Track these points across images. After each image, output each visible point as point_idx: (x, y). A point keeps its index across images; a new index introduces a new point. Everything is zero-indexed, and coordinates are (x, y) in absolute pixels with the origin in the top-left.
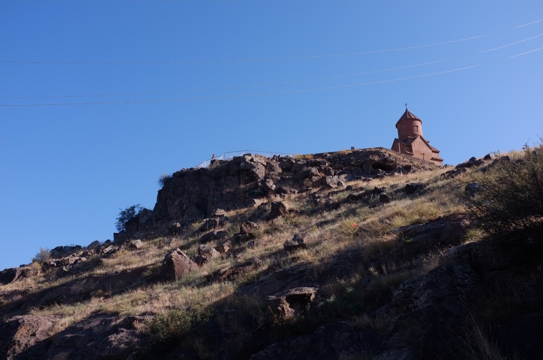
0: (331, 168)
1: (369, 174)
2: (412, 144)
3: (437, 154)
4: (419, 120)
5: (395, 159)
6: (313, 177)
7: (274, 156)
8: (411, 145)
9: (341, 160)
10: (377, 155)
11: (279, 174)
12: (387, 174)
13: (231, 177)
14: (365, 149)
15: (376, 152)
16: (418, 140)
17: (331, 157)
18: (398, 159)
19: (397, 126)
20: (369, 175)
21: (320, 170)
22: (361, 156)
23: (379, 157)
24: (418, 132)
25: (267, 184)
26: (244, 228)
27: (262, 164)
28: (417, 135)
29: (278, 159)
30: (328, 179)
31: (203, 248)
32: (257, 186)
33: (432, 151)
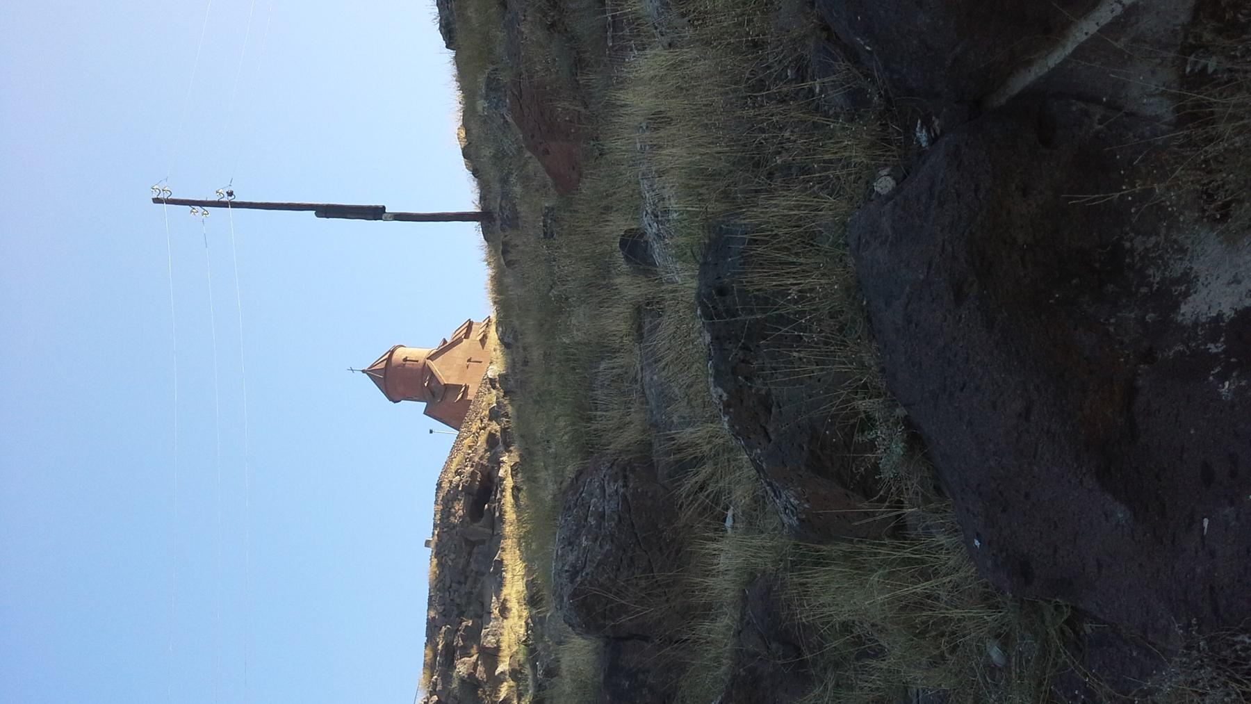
0: (464, 624)
1: (493, 532)
3: (474, 326)
4: (392, 352)
5: (470, 461)
6: (477, 675)
8: (445, 384)
9: (450, 587)
10: (453, 503)
12: (498, 496)
14: (435, 526)
15: (446, 504)
16: (434, 365)
18: (469, 454)
19: (395, 402)
20: (495, 533)
23: (460, 500)
24: (417, 361)
28: (425, 363)
30: (489, 642)
33: (465, 338)
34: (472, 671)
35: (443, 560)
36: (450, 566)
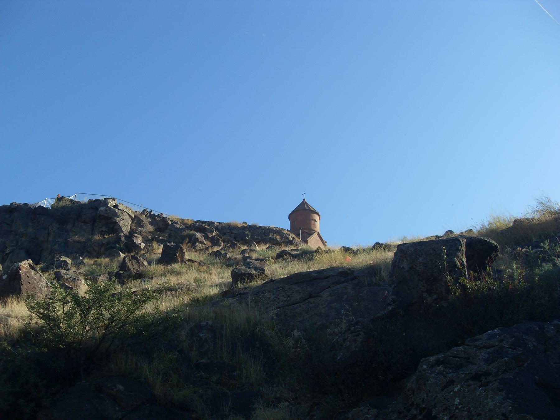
2: (308, 239)
4: (318, 214)
6: (198, 243)
7: (144, 209)
8: (307, 241)
10: (279, 235)
11: (150, 232)
13: (82, 224)
16: (315, 236)
17: (220, 226)
21: (206, 238)
22: (258, 232)
24: (315, 227)
25: (135, 240)
26: (129, 264)
27: (128, 214)
28: (314, 231)
29: (148, 215)
31: (65, 274)
32: (118, 240)
34: (200, 240)
35: (248, 230)
36: (244, 233)
